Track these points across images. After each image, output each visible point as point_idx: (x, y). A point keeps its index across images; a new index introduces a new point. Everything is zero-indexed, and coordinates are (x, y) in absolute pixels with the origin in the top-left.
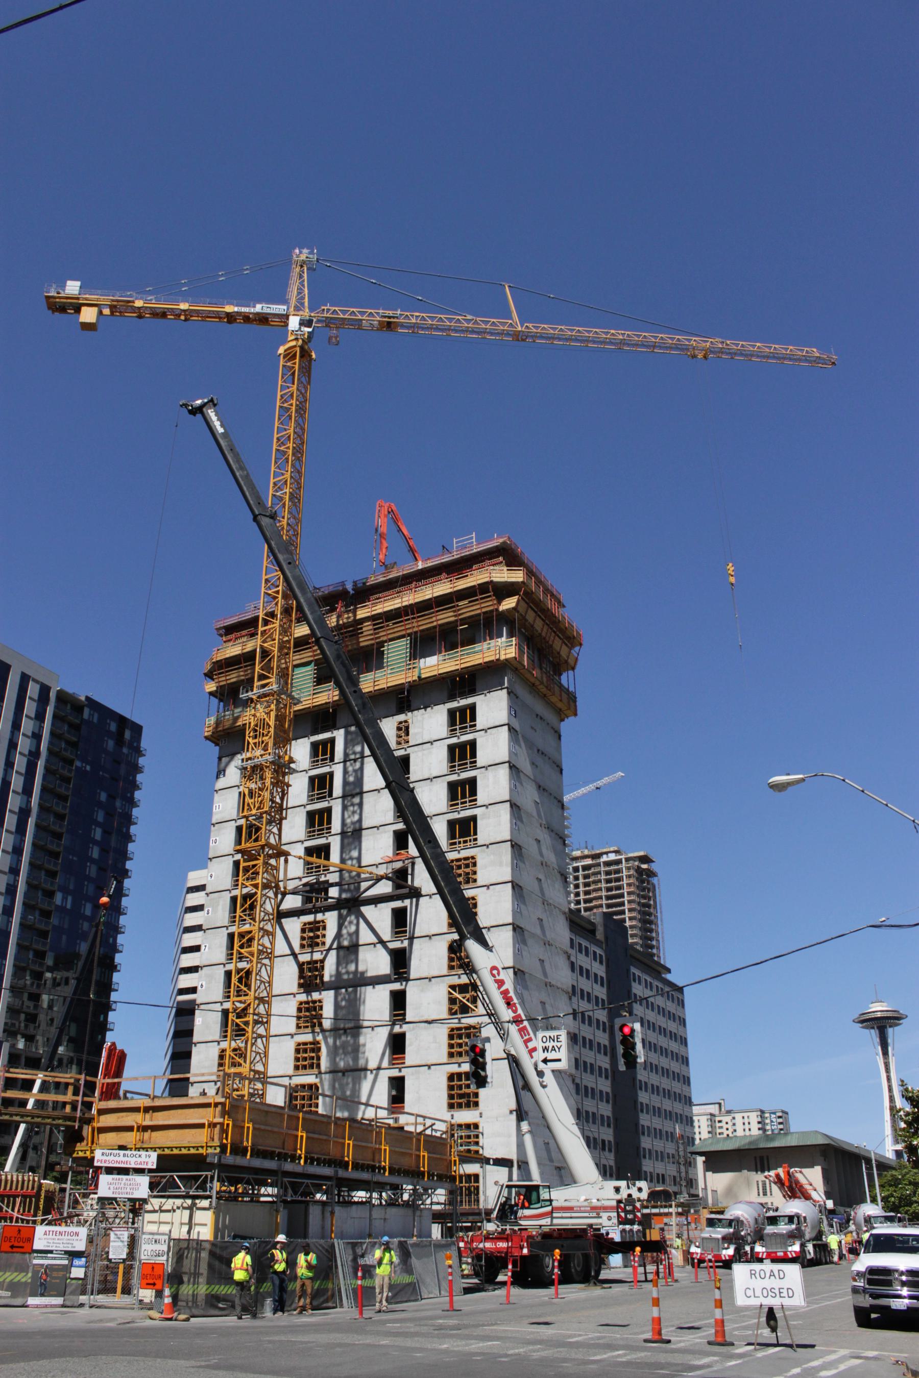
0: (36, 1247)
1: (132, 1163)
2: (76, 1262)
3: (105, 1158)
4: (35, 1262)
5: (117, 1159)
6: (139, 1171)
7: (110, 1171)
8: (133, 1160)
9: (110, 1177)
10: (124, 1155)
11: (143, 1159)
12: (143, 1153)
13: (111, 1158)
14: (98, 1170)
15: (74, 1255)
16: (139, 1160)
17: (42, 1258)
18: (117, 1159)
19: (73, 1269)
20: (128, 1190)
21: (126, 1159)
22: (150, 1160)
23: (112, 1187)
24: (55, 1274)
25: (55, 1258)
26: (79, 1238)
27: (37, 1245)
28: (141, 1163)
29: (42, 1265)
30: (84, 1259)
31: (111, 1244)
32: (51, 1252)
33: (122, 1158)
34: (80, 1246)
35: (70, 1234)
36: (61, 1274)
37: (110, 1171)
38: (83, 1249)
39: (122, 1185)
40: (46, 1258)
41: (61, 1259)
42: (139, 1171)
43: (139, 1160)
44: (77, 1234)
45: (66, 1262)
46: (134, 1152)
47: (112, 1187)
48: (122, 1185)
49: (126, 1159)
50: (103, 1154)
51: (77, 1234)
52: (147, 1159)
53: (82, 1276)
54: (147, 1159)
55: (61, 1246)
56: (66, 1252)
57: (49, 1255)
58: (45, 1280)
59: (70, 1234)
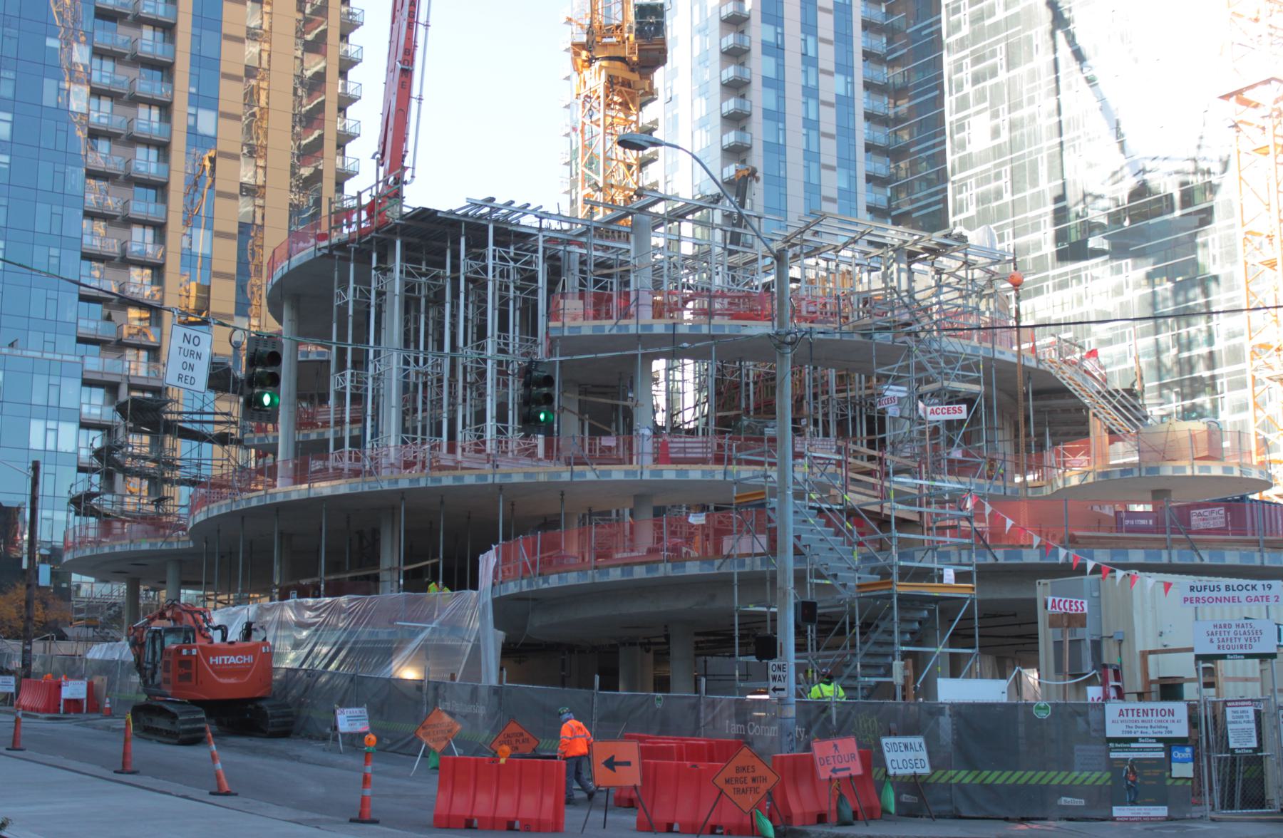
0: (1109, 734)
2: (1177, 754)
4: (1113, 755)
10: (1227, 588)
12: (1259, 583)
15: (1170, 743)
17: (1123, 750)
19: (1174, 765)
20: (1243, 642)
23: (1215, 638)
24: (1147, 773)
25: (1143, 750)
26: (1176, 718)
27: (1113, 730)
29: (1125, 760)
30: (1188, 750)
31: (1230, 727)
32: (1135, 740)
34: (1181, 730)
35: (1161, 712)
36: (1156, 772)
38: (1185, 734)
39: (1232, 635)
40: (1130, 750)
41: (1153, 750)
44: (1172, 713)
45: (1162, 755)
47: (1215, 638)
48: (1232, 635)
51: (1172, 713)
52: (1267, 592)
53: (1191, 775)
54: (1267, 592)
55: (1150, 730)
56: (1159, 740)
57: (1133, 745)
58: (1134, 782)
59: (1161, 712)
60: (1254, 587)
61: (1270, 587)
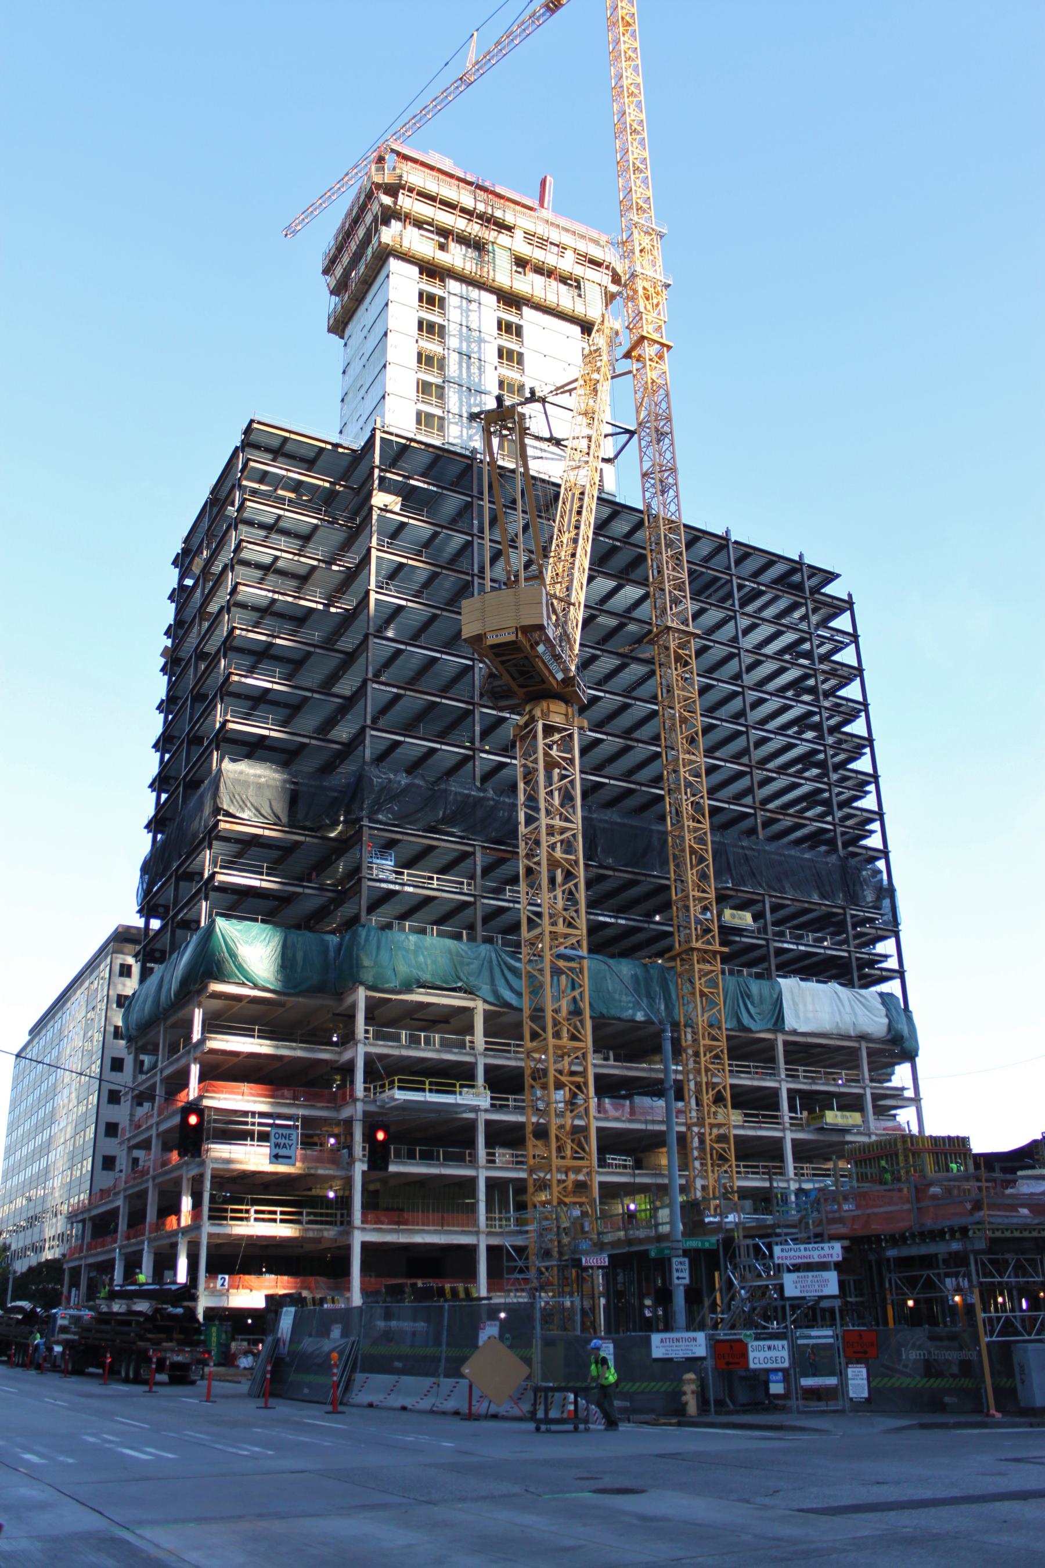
1: (816, 1256)
3: (784, 1254)
5: (798, 1254)
6: (822, 1266)
7: (797, 1268)
8: (815, 1254)
9: (794, 1276)
10: (805, 1249)
11: (827, 1251)
13: (792, 1253)
14: (779, 1268)
16: (822, 1253)
18: (798, 1254)
20: (817, 1287)
21: (808, 1253)
22: (834, 1251)
28: (825, 1256)
33: (803, 1253)
37: (797, 1268)
42: (822, 1266)
43: (822, 1253)
46: (816, 1246)
49: (808, 1253)
50: (782, 1250)
52: (831, 1252)
54: (831, 1252)
60: (822, 1248)
61: (833, 1248)
